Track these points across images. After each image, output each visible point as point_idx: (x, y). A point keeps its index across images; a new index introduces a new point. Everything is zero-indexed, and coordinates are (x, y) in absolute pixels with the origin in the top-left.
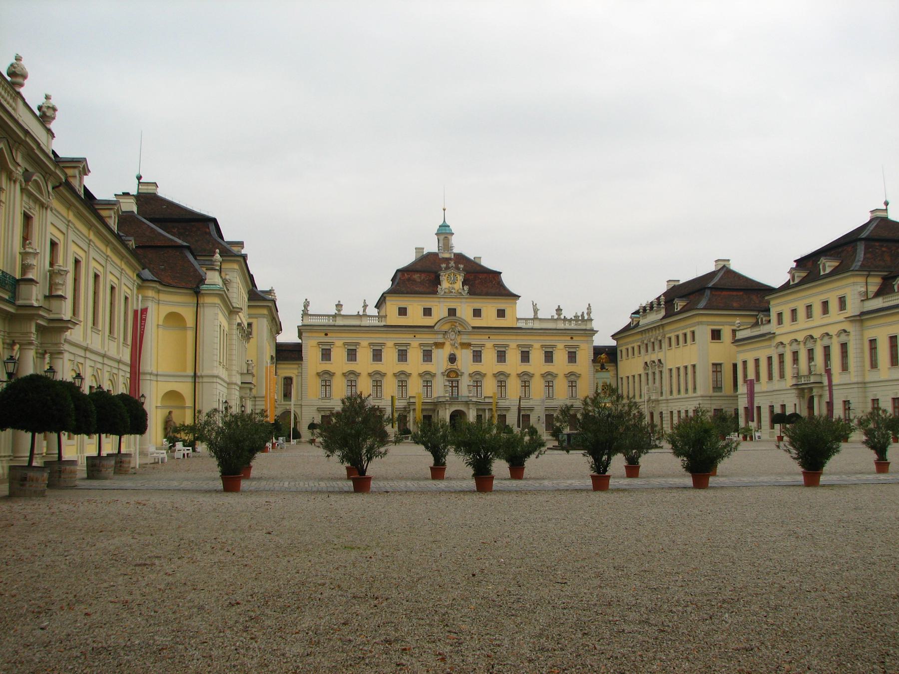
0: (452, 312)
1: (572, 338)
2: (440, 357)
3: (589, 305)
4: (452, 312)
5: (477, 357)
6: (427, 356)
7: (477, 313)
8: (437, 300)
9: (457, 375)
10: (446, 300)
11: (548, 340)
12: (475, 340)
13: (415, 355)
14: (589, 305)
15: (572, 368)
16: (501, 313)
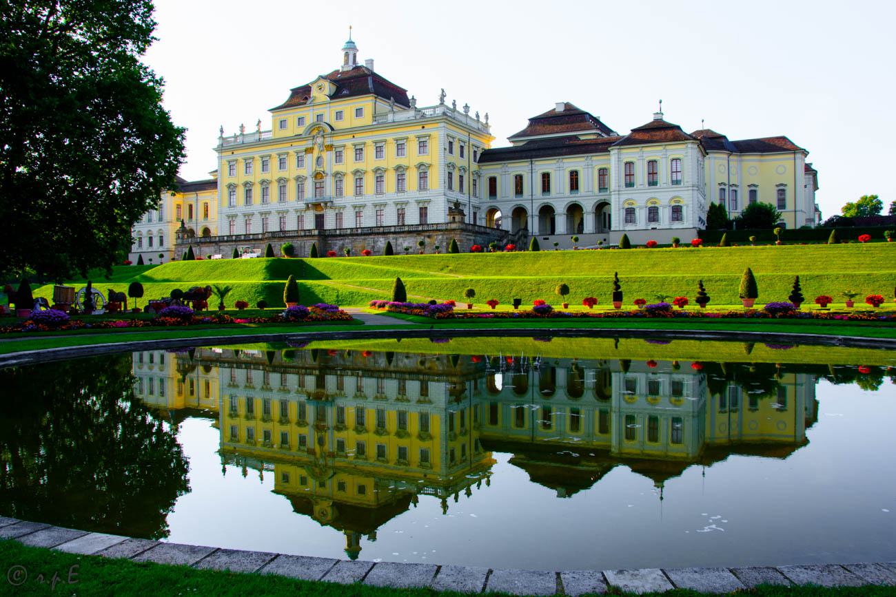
0: (319, 117)
1: (423, 127)
2: (310, 160)
3: (443, 91)
4: (319, 117)
5: (339, 157)
6: (300, 161)
7: (339, 115)
8: (308, 109)
9: (322, 178)
10: (315, 108)
11: (401, 132)
12: (337, 141)
13: (292, 162)
14: (443, 91)
15: (425, 159)
16: (359, 112)
